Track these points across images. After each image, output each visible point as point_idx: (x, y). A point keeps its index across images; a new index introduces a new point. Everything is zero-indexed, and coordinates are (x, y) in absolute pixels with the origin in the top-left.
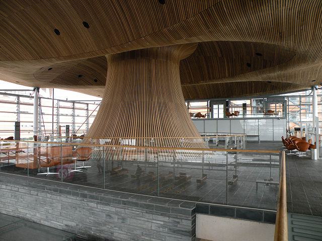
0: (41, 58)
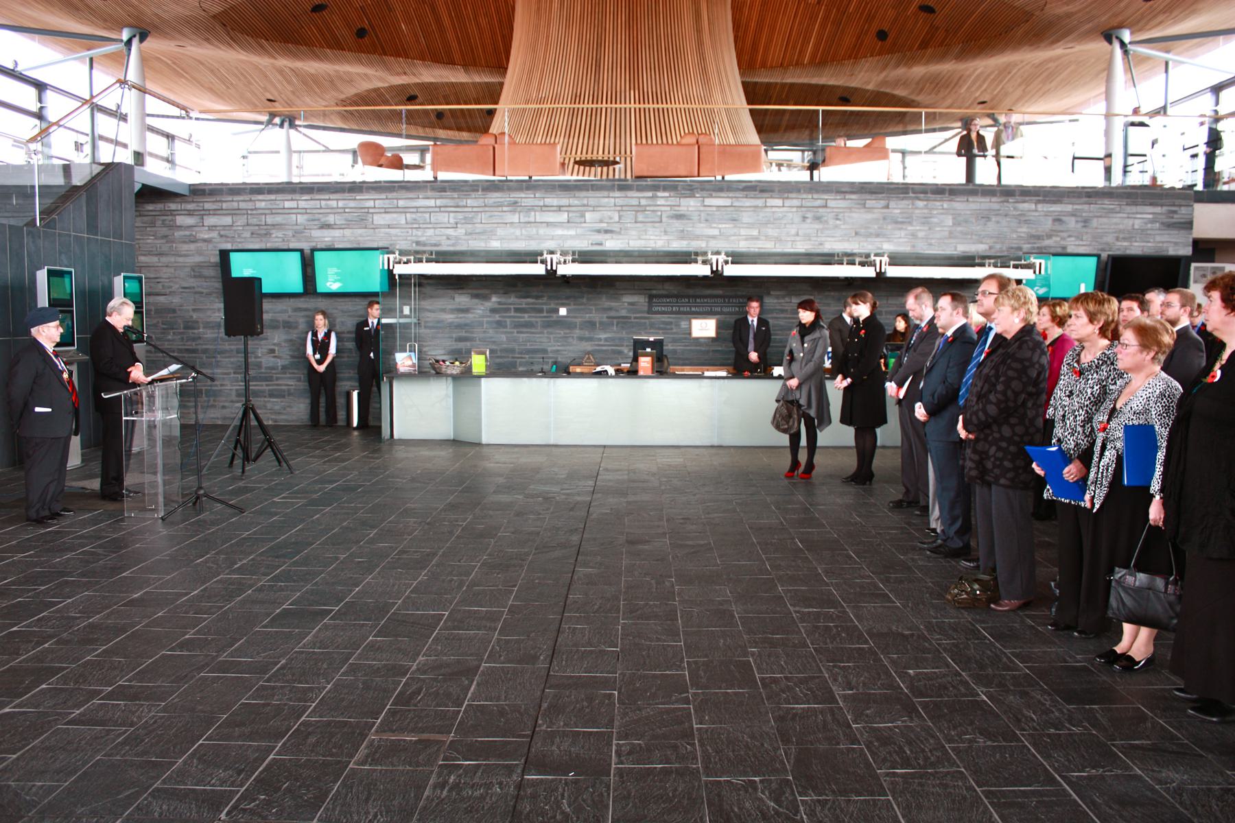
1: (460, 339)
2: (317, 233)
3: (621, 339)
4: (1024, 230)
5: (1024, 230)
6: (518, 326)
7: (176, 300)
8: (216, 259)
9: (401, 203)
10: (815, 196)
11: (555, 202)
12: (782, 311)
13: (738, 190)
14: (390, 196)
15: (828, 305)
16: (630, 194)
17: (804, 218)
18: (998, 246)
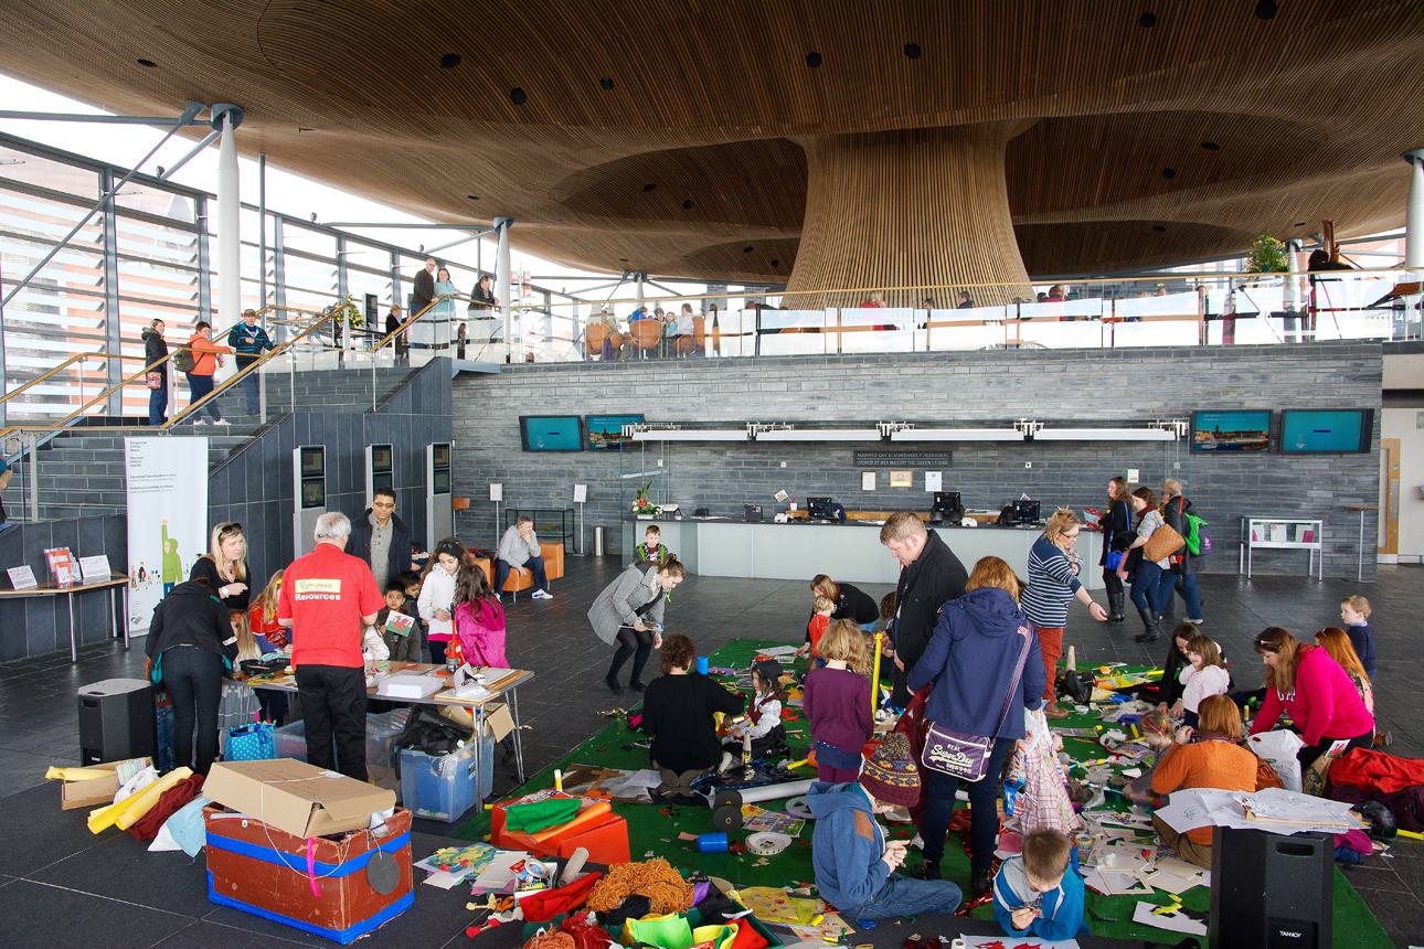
0: (721, 122)
1: (701, 487)
2: (592, 402)
3: (831, 488)
4: (1199, 388)
5: (1199, 388)
6: (747, 476)
7: (491, 454)
8: (518, 423)
9: (657, 377)
10: (998, 363)
11: (777, 374)
12: (971, 464)
13: (929, 360)
14: (648, 371)
15: (1011, 458)
16: (837, 366)
17: (989, 383)
18: (1173, 403)
